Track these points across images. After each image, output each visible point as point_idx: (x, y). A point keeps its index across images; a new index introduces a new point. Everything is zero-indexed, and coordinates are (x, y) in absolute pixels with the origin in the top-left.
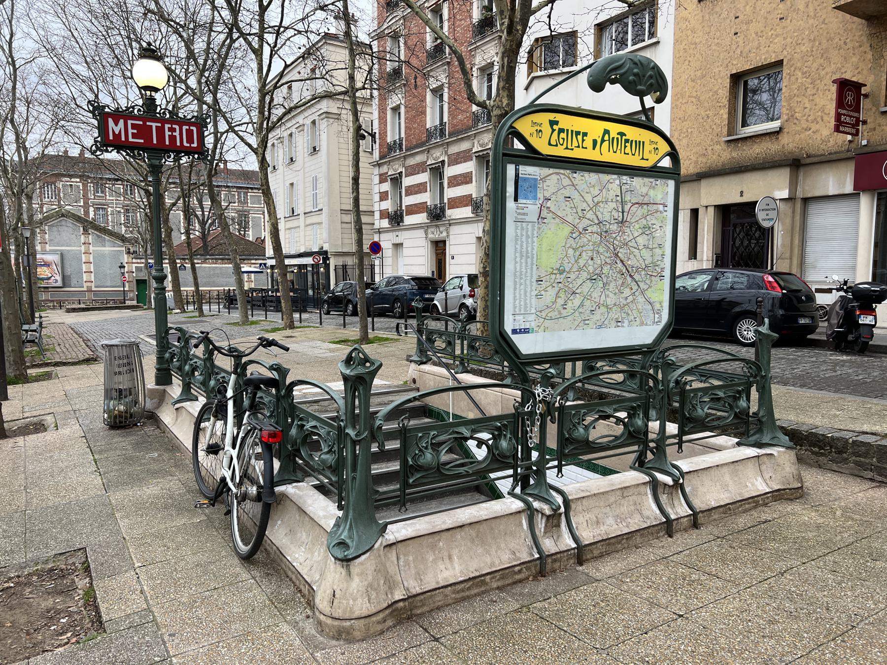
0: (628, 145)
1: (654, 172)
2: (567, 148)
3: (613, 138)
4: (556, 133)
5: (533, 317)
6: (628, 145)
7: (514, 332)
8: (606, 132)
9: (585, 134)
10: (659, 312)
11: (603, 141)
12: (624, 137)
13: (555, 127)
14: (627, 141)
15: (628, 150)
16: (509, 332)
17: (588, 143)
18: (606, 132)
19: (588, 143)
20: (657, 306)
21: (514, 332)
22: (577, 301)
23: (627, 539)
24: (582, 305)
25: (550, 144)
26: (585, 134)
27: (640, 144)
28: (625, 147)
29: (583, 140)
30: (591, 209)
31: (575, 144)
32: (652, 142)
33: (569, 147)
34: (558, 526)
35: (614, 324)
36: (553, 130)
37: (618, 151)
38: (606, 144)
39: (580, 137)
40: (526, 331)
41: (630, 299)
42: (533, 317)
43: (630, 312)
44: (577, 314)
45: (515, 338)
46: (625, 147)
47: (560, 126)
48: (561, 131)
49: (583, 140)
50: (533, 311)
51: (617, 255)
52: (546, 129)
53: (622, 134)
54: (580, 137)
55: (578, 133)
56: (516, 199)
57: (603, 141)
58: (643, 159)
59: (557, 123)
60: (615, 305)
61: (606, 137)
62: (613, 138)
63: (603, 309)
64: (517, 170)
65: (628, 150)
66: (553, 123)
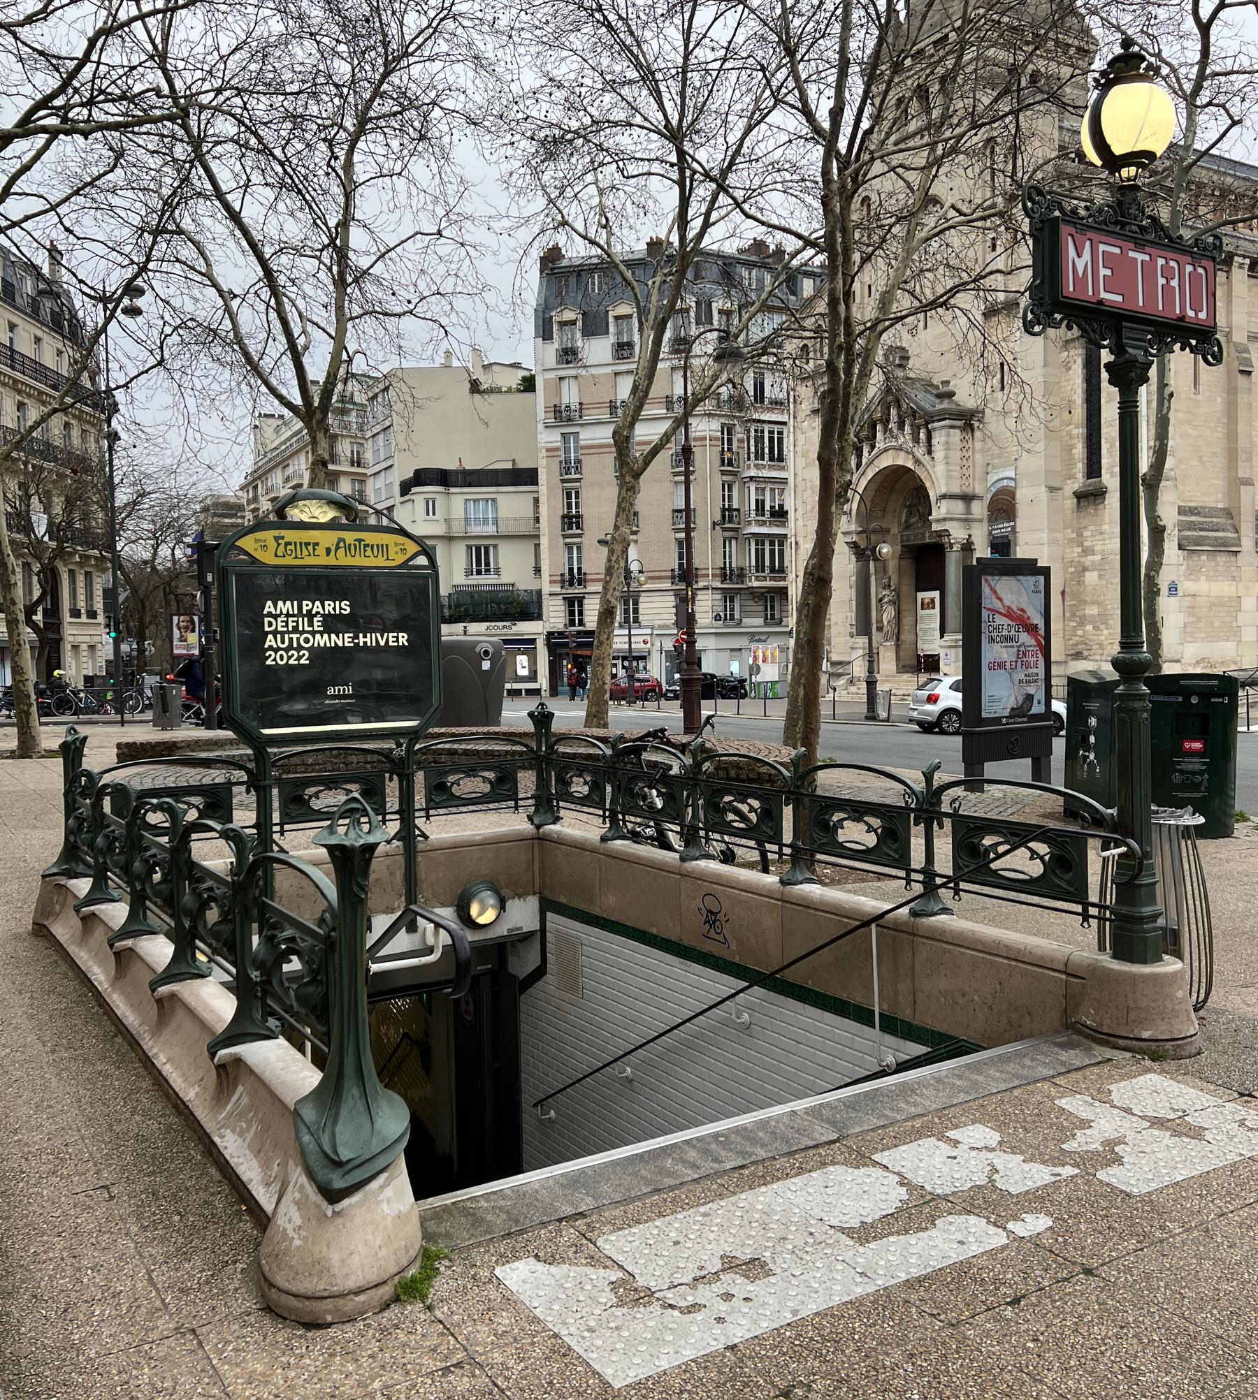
0: (369, 549)
4: (282, 547)
6: (369, 549)
9: (317, 544)
11: (337, 548)
14: (366, 546)
15: (369, 553)
18: (341, 540)
19: (321, 550)
26: (317, 544)
27: (383, 548)
31: (305, 552)
32: (397, 544)
36: (279, 545)
38: (341, 552)
39: (310, 548)
48: (287, 544)
53: (360, 540)
55: (307, 544)
57: (337, 548)
59: (283, 538)
61: (342, 544)
65: (369, 553)
66: (276, 539)
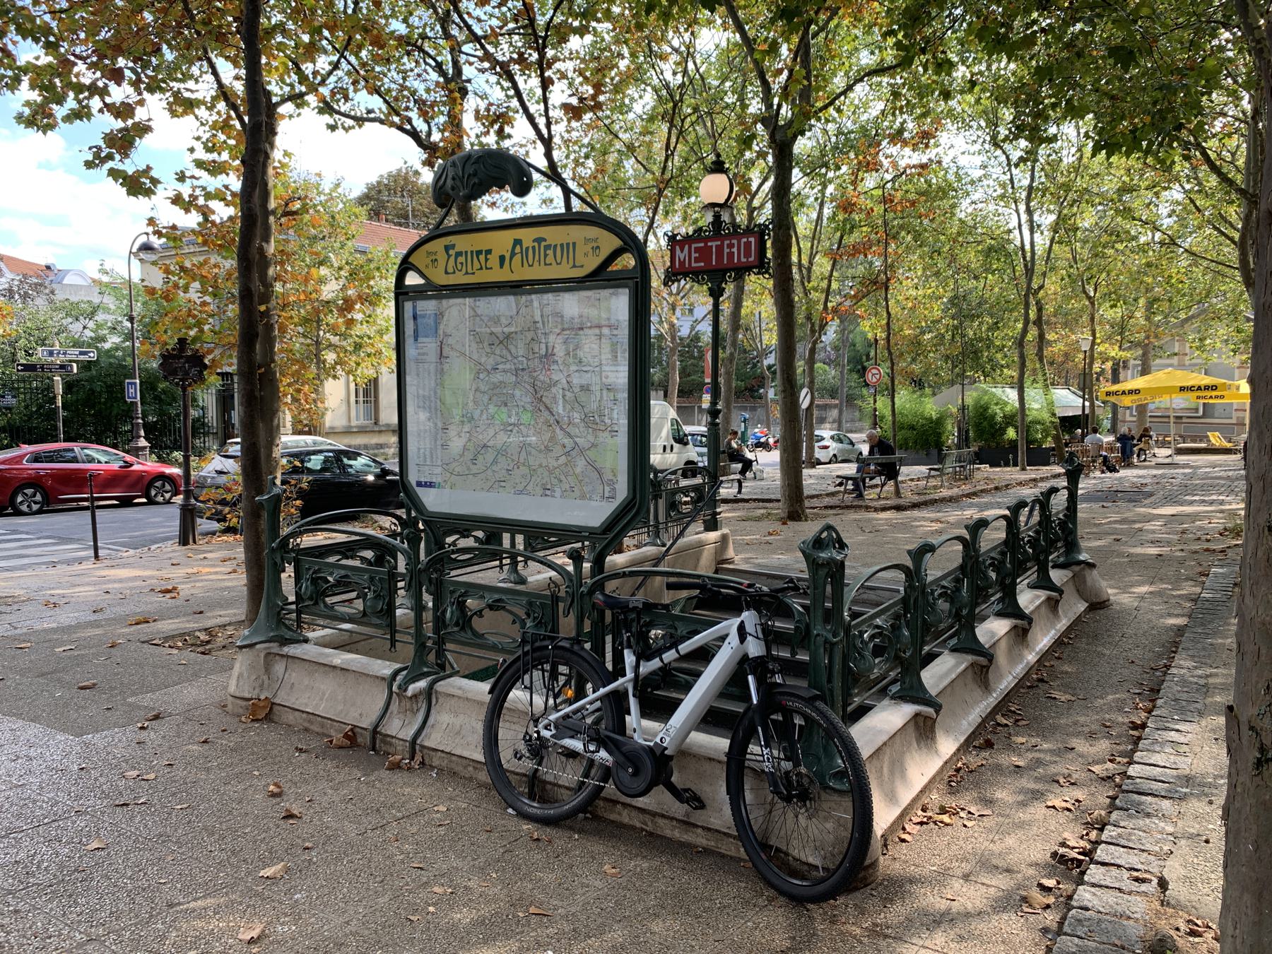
0: (550, 252)
1: (600, 277)
2: (467, 273)
3: (527, 249)
5: (439, 470)
6: (550, 252)
7: (419, 484)
8: (518, 242)
9: (489, 252)
10: (612, 483)
11: (513, 254)
12: (543, 244)
13: (451, 252)
15: (550, 259)
16: (414, 484)
17: (494, 260)
18: (518, 242)
19: (494, 260)
20: (608, 475)
21: (419, 484)
22: (490, 456)
23: (475, 768)
24: (495, 462)
25: (446, 273)
26: (489, 252)
27: (569, 248)
28: (546, 255)
29: (487, 260)
30: (501, 342)
31: (477, 265)
32: (587, 240)
33: (470, 271)
34: (415, 713)
35: (539, 491)
36: (449, 256)
37: (536, 263)
38: (518, 258)
39: (482, 257)
40: (430, 485)
41: (563, 460)
42: (439, 470)
43: (562, 477)
44: (489, 472)
45: (420, 491)
46: (546, 255)
47: (457, 249)
48: (459, 254)
49: (487, 260)
50: (439, 463)
51: (540, 400)
52: (442, 257)
53: (539, 240)
54: (482, 257)
55: (479, 253)
56: (416, 339)
57: (513, 254)
58: (574, 266)
59: (453, 246)
60: (540, 466)
61: (518, 249)
62: (527, 249)
63: (524, 470)
64: (414, 308)
65: (550, 259)
